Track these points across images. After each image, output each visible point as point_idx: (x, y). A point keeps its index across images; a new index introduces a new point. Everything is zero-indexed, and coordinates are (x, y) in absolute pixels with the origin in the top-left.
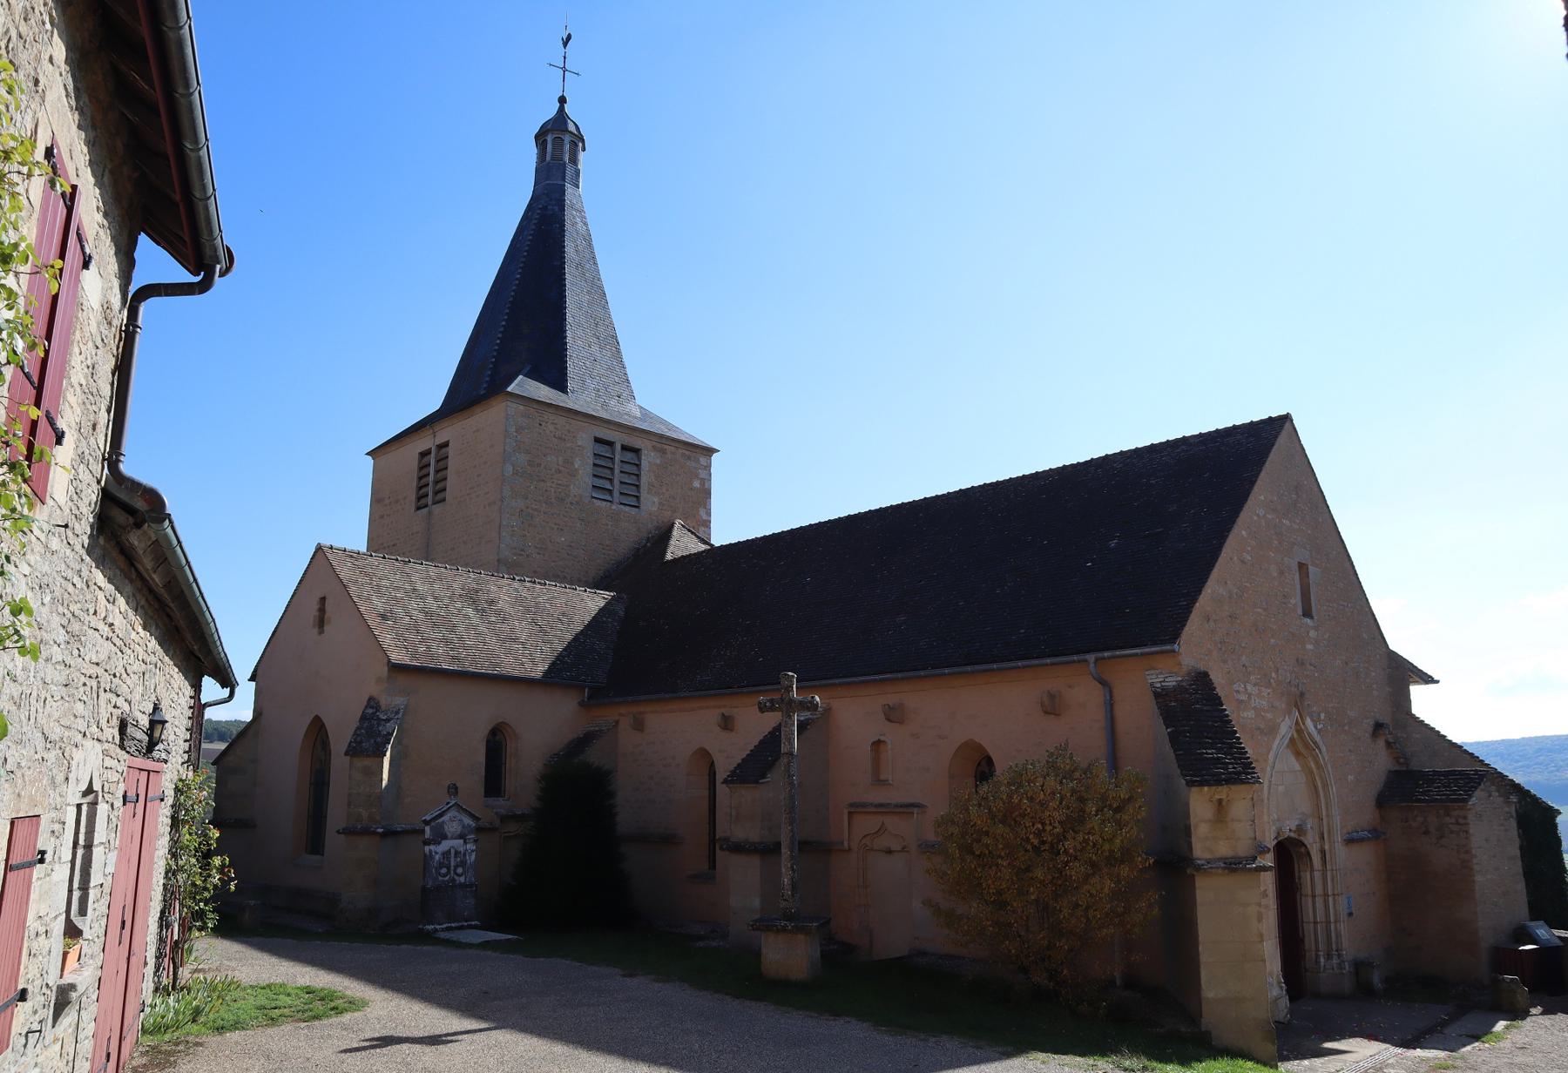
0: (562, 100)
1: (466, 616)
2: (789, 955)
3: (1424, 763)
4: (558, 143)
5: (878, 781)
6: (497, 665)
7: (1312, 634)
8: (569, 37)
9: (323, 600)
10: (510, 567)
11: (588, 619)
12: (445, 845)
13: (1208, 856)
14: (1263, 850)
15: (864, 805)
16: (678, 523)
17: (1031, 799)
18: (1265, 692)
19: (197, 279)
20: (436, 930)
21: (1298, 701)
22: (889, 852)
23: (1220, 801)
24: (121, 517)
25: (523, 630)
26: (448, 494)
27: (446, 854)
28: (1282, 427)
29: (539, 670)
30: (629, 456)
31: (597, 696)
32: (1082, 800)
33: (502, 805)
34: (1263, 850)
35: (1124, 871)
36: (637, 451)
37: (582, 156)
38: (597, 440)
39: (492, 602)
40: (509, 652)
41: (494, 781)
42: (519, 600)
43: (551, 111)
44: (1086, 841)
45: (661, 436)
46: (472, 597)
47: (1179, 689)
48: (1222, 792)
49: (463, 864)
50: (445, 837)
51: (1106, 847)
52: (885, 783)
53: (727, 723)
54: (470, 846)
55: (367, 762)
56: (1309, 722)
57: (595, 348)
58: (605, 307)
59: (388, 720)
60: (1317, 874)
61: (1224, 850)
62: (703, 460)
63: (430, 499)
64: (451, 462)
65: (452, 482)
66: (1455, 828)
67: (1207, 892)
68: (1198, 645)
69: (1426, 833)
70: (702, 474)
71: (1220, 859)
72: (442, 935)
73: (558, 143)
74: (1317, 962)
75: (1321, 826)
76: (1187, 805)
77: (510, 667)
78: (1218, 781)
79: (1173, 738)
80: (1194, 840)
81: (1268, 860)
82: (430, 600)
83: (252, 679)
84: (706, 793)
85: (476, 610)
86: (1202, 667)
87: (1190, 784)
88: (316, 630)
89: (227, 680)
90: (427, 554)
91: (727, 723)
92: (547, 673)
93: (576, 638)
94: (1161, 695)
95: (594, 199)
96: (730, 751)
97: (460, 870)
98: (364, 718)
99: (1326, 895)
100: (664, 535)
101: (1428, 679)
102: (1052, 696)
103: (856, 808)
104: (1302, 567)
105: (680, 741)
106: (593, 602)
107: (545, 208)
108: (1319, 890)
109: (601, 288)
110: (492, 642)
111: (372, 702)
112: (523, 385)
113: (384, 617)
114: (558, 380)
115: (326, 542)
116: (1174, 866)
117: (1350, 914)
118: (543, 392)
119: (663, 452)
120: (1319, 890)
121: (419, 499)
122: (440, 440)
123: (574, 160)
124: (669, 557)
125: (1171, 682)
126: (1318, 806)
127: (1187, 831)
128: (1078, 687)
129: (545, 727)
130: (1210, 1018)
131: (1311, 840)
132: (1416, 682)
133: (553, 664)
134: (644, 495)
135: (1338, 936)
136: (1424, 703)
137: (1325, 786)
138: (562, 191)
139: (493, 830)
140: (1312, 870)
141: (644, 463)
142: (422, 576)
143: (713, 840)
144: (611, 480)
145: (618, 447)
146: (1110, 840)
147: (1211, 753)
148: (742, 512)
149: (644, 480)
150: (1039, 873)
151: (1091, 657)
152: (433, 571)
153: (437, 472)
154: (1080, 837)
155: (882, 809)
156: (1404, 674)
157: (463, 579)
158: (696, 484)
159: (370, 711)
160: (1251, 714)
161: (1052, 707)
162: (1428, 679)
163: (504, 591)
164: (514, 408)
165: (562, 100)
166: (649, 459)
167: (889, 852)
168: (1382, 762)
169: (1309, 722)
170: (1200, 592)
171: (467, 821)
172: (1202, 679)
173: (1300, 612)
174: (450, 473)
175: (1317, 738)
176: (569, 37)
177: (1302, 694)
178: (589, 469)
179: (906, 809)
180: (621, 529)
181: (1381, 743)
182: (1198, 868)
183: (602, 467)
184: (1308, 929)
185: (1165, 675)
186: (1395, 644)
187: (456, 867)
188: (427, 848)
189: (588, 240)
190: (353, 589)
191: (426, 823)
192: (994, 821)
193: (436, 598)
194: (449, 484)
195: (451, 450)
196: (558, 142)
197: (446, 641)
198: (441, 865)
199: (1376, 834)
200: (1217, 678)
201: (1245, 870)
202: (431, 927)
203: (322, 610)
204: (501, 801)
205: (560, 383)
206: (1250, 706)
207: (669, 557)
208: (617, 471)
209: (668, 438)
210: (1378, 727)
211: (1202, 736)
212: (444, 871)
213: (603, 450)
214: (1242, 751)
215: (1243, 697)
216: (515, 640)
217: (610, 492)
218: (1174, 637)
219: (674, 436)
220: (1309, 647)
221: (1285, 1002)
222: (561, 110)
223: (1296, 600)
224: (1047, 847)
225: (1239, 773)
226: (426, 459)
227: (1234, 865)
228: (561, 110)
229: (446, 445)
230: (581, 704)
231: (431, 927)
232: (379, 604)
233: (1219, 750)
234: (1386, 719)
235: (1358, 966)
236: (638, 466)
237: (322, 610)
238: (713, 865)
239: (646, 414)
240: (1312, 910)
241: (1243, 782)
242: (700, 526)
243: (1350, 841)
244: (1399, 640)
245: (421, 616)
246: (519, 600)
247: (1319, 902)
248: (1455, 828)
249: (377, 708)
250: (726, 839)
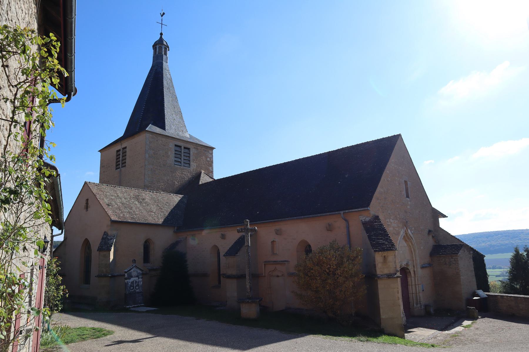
0: (161, 34)
1: (136, 204)
2: (250, 310)
3: (444, 243)
4: (160, 48)
6: (147, 220)
7: (409, 203)
8: (164, 14)
9: (87, 200)
10: (146, 187)
11: (175, 204)
12: (132, 279)
13: (382, 274)
14: (397, 271)
15: (269, 262)
16: (203, 171)
17: (326, 258)
18: (396, 221)
20: (130, 308)
21: (406, 224)
23: (385, 256)
25: (154, 208)
26: (127, 164)
27: (132, 282)
28: (398, 138)
29: (161, 221)
30: (186, 151)
31: (179, 229)
32: (342, 257)
34: (397, 271)
35: (356, 279)
36: (189, 149)
37: (168, 52)
38: (176, 146)
39: (144, 199)
40: (150, 215)
41: (146, 258)
42: (152, 198)
43: (158, 38)
44: (344, 270)
45: (197, 144)
46: (137, 198)
47: (370, 222)
48: (385, 253)
49: (138, 285)
51: (350, 272)
53: (223, 237)
54: (140, 280)
55: (105, 253)
56: (409, 230)
57: (174, 115)
58: (177, 102)
59: (111, 239)
60: (413, 278)
61: (386, 271)
62: (210, 152)
63: (120, 166)
64: (128, 154)
65: (128, 161)
66: (454, 262)
67: (381, 285)
68: (375, 208)
69: (446, 264)
70: (210, 156)
71: (385, 275)
72: (132, 309)
73: (160, 48)
74: (414, 306)
75: (413, 263)
76: (374, 258)
77: (151, 220)
78: (384, 250)
79: (369, 237)
80: (377, 269)
81: (398, 274)
82: (123, 199)
85: (139, 202)
86: (377, 214)
87: (375, 251)
88: (85, 210)
91: (223, 237)
92: (164, 222)
93: (172, 211)
94: (364, 224)
95: (172, 66)
96: (225, 246)
97: (137, 288)
98: (103, 238)
99: (416, 285)
100: (199, 176)
101: (444, 216)
102: (329, 225)
103: (267, 263)
104: (406, 182)
105: (207, 242)
106: (176, 198)
107: (156, 70)
108: (413, 283)
109: (176, 96)
110: (145, 212)
111: (105, 233)
112: (151, 128)
113: (108, 205)
114: (162, 126)
115: (88, 181)
116: (371, 277)
117: (423, 290)
118: (158, 130)
119: (197, 149)
120: (413, 283)
123: (166, 54)
124: (200, 183)
125: (367, 219)
126: (412, 257)
127: (375, 266)
128: (338, 221)
129: (163, 240)
130: (383, 325)
131: (411, 268)
132: (441, 217)
133: (165, 219)
134: (192, 163)
135: (420, 297)
136: (443, 224)
137: (414, 250)
138: (162, 64)
140: (411, 277)
141: (191, 153)
142: (120, 191)
143: (219, 275)
144: (181, 159)
145: (183, 148)
146: (351, 270)
147: (381, 241)
148: (224, 168)
149: (191, 158)
150: (329, 281)
151: (342, 212)
152: (124, 190)
153: (123, 157)
154: (342, 269)
156: (437, 215)
157: (133, 192)
158: (208, 159)
159: (105, 236)
160: (392, 229)
161: (330, 228)
162: (444, 216)
163: (147, 195)
164: (148, 135)
165: (161, 34)
166: (193, 151)
167: (278, 276)
168: (431, 242)
169: (409, 230)
170: (375, 191)
171: (139, 271)
172: (377, 218)
173: (405, 196)
174: (127, 157)
175: (412, 236)
176: (164, 14)
177: (407, 222)
178: (174, 155)
179: (283, 263)
180: (184, 175)
181: (431, 237)
182: (379, 278)
183: (178, 154)
184: (410, 296)
185: (365, 217)
186: (434, 205)
187: (136, 286)
188: (126, 281)
189: (171, 80)
190: (98, 196)
191: (126, 272)
192: (312, 265)
193: (125, 199)
194: (127, 161)
195: (127, 150)
196: (160, 48)
197: (129, 212)
198: (131, 286)
199: (430, 265)
200: (381, 217)
201: (393, 277)
202: (128, 307)
203: (87, 203)
204: (149, 265)
205: (163, 127)
206: (391, 225)
207: (200, 183)
208: (182, 156)
209: (199, 144)
210: (430, 231)
211: (377, 236)
212: (132, 288)
213: (178, 149)
214: (391, 240)
215: (389, 223)
216: (152, 212)
217: (180, 162)
218: (368, 205)
219: (201, 144)
220: (408, 207)
221: (404, 319)
222: (161, 37)
223: (404, 193)
224: (331, 272)
225: (390, 247)
227: (390, 276)
228: (161, 37)
229: (126, 148)
230: (174, 232)
231: (128, 307)
232: (106, 201)
233: (384, 240)
234: (432, 229)
235: (426, 306)
236: (189, 154)
237: (87, 203)
239: (191, 137)
240: (412, 289)
241: (392, 250)
242: (210, 173)
243: (422, 267)
244: (436, 204)
245: (121, 204)
246: (152, 198)
247: (414, 287)
248: (454, 262)
249: (107, 235)
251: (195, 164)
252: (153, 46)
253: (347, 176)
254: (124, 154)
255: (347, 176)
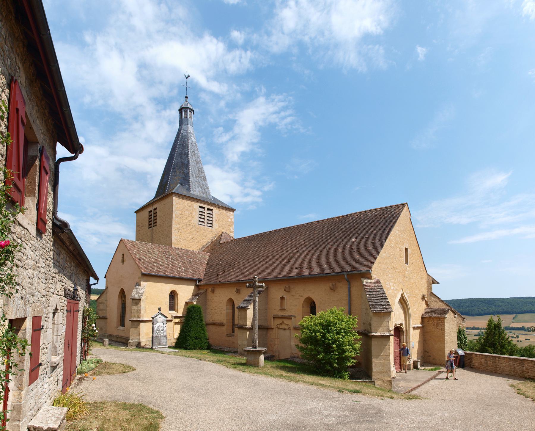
5: (282, 309)
9: (123, 255)
19: (73, 155)
22: (285, 329)
24: (58, 230)
30: (210, 212)
33: (174, 313)
36: (211, 210)
38: (200, 207)
40: (175, 269)
50: (158, 322)
52: (285, 310)
65: (158, 221)
83: (105, 278)
84: (232, 311)
88: (121, 264)
89: (96, 278)
90: (152, 242)
115: (123, 238)
121: (149, 225)
122: (154, 207)
139: (171, 321)
142: (150, 246)
145: (206, 209)
149: (214, 219)
153: (154, 217)
155: (283, 317)
158: (229, 220)
194: (157, 221)
203: (123, 258)
226: (150, 214)
237: (123, 258)
238: (234, 332)
250: (237, 325)
251: (217, 225)
252: (179, 110)
253: (353, 240)
254: (155, 215)
255: (353, 240)
